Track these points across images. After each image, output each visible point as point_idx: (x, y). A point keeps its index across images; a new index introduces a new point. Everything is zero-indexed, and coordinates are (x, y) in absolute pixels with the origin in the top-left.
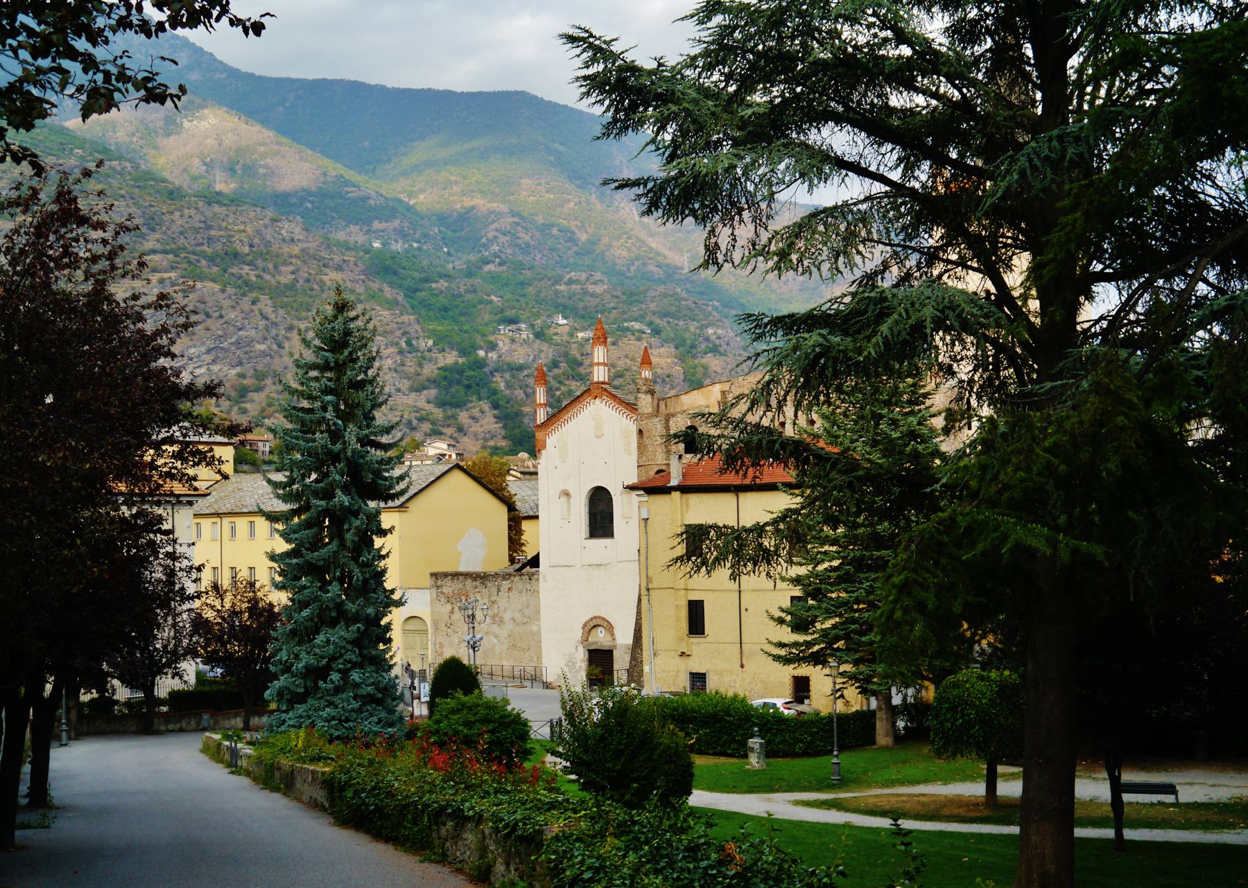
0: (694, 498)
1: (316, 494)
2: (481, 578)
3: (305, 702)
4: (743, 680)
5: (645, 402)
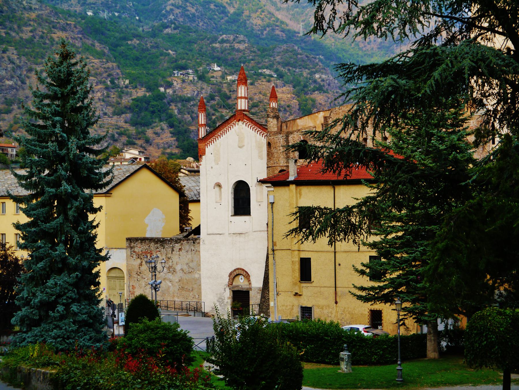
0: (305, 190)
1: (49, 184)
2: (161, 242)
3: (40, 326)
4: (337, 312)
5: (273, 124)
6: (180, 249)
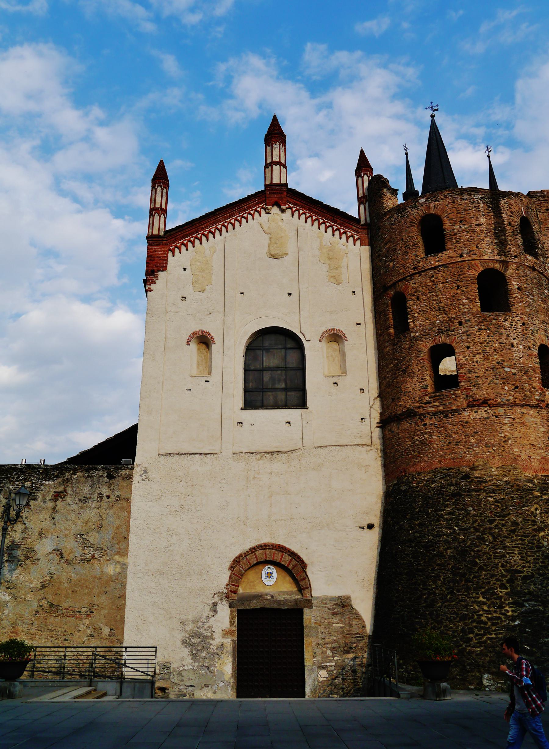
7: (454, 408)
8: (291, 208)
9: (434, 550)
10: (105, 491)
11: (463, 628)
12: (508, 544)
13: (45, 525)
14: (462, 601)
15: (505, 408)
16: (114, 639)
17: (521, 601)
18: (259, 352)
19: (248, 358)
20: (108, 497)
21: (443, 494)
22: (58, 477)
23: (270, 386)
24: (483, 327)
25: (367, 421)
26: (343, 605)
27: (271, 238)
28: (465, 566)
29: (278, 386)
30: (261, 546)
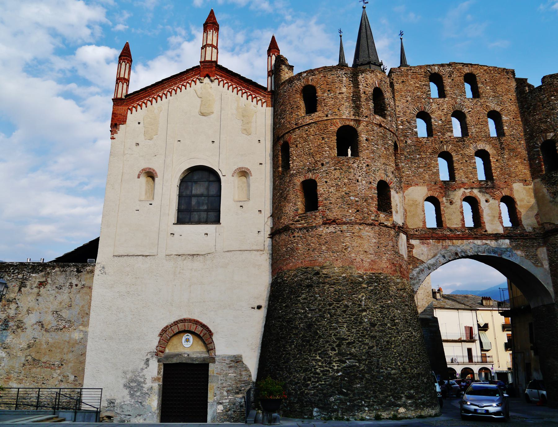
6: (41, 284)
7: (314, 225)
8: (218, 79)
9: (292, 324)
10: (75, 281)
11: (305, 377)
12: (340, 320)
13: (32, 304)
14: (306, 359)
15: (348, 225)
16: (77, 383)
17: (344, 359)
18: (190, 184)
19: (181, 188)
20: (76, 285)
21: (301, 285)
22: (41, 271)
23: (196, 208)
24: (338, 168)
25: (262, 233)
26: (237, 361)
27: (202, 101)
28: (310, 335)
29: (201, 208)
30: (182, 320)
